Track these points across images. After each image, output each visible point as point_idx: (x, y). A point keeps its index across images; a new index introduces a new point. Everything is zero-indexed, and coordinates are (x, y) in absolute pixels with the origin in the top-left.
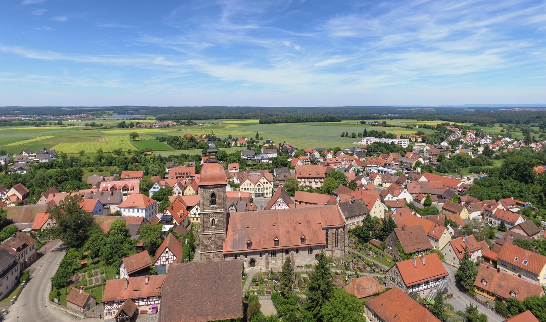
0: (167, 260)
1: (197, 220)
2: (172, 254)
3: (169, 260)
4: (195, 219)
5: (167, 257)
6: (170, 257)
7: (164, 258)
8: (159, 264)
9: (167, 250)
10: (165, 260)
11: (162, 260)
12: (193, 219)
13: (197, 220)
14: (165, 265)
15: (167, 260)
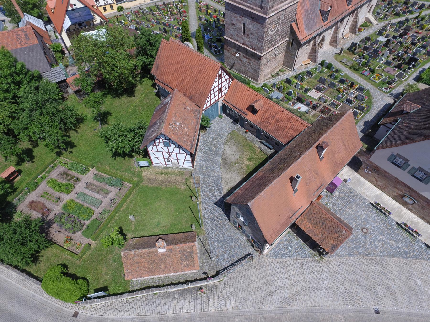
0: (220, 90)
1: (112, 8)
2: (227, 77)
3: (223, 89)
4: (108, 7)
5: (220, 87)
6: (224, 84)
7: (216, 89)
8: (209, 104)
9: (220, 73)
10: (216, 94)
11: (212, 96)
12: (105, 9)
13: (112, 8)
14: (217, 102)
15: (220, 90)
